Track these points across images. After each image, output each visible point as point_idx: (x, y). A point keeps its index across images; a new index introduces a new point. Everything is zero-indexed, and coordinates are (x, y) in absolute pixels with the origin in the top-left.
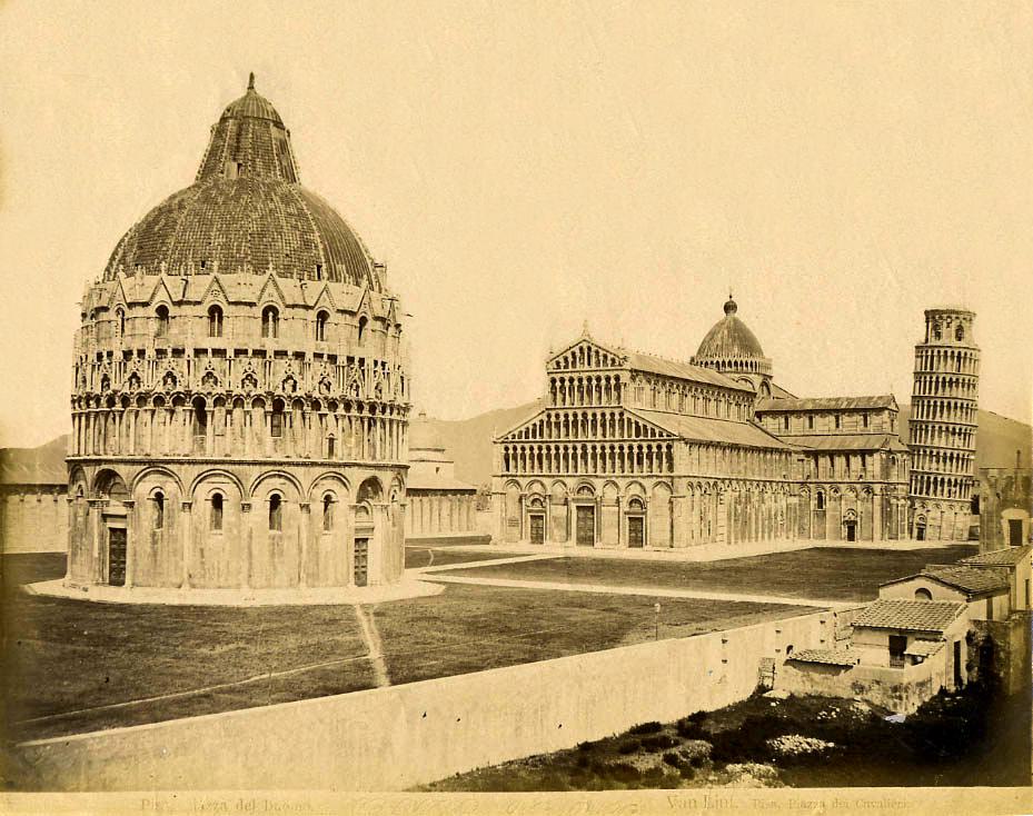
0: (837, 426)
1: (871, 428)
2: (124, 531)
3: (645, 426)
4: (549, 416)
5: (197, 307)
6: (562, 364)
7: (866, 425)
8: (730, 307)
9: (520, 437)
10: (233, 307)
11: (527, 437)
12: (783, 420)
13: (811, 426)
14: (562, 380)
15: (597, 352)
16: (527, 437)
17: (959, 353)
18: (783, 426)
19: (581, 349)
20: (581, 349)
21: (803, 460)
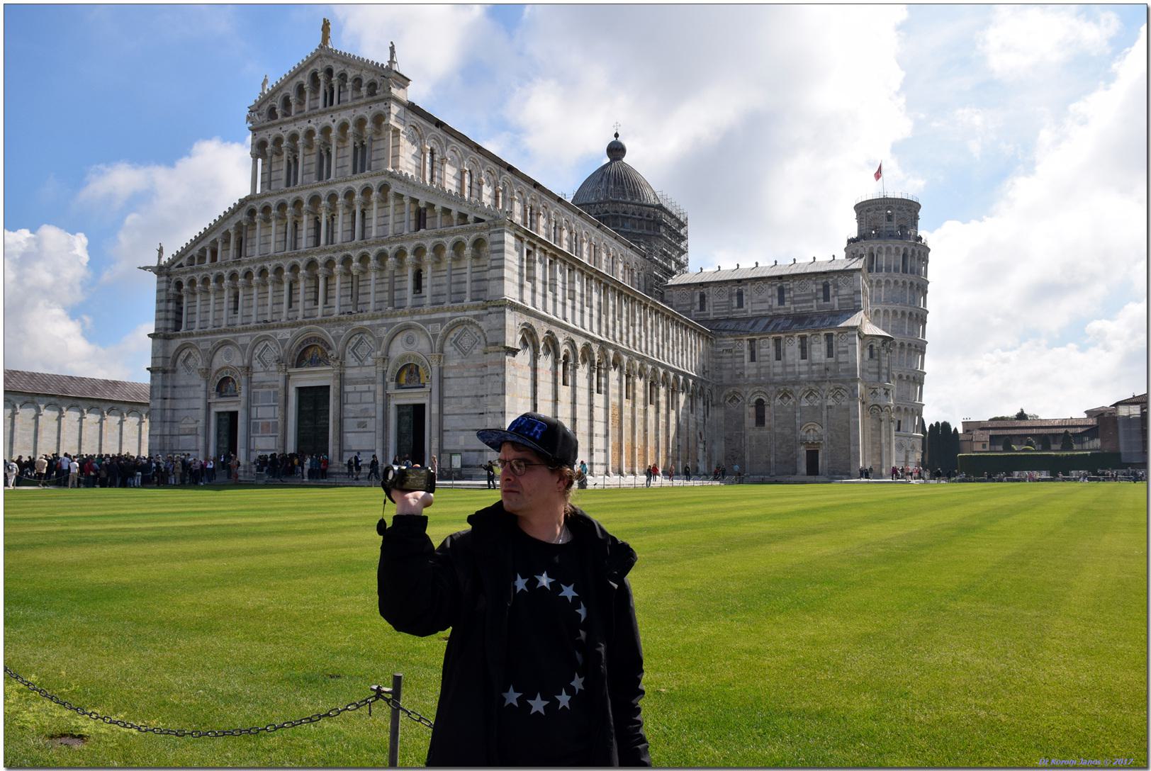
0: (781, 301)
1: (835, 302)
3: (432, 206)
4: (252, 212)
6: (278, 111)
7: (826, 298)
8: (616, 150)
9: (202, 259)
11: (214, 259)
12: (697, 299)
13: (740, 305)
14: (278, 141)
15: (343, 76)
16: (214, 259)
17: (905, 250)
18: (698, 307)
19: (314, 76)
21: (730, 351)
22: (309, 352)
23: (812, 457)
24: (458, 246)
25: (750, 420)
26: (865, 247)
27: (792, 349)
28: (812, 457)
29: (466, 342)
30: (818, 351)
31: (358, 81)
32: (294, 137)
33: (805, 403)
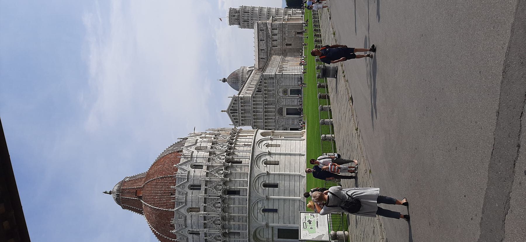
0: (264, 40)
2: (279, 230)
4: (255, 126)
5: (188, 194)
8: (224, 80)
10: (190, 180)
14: (242, 120)
15: (232, 107)
19: (231, 113)
20: (231, 113)
22: (280, 112)
23: (298, 33)
24: (265, 83)
25: (290, 47)
26: (242, 22)
27: (275, 37)
28: (298, 33)
29: (280, 82)
30: (276, 32)
31: (234, 104)
32: (242, 117)
33: (287, 35)
